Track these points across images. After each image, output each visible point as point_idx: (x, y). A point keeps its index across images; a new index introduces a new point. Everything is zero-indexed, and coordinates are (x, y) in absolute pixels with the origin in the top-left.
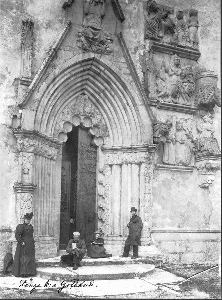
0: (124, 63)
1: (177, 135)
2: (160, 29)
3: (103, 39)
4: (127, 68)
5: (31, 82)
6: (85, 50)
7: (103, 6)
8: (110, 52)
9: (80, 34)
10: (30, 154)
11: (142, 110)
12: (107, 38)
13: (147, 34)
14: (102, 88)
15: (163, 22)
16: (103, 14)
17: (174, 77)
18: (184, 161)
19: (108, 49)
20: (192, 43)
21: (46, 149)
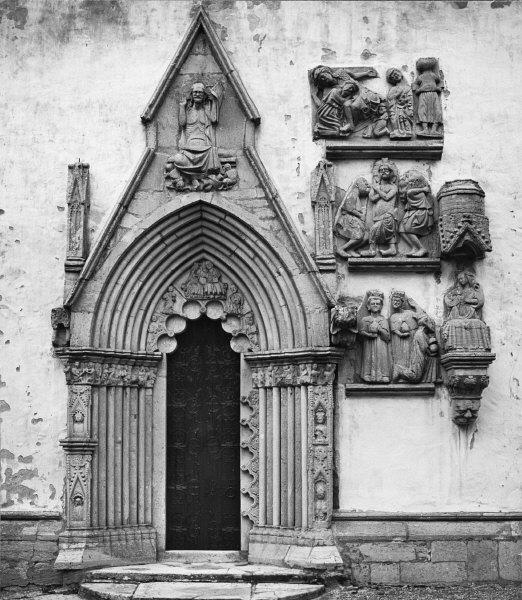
0: (260, 198)
1: (392, 319)
2: (343, 116)
3: (214, 162)
4: (268, 207)
5: (82, 266)
6: (180, 190)
7: (214, 106)
8: (232, 184)
9: (169, 166)
10: (84, 388)
11: (302, 282)
12: (225, 160)
13: (316, 130)
14: (233, 248)
15: (347, 103)
16: (214, 120)
17: (380, 203)
18: (407, 372)
19: (225, 180)
20: (425, 125)
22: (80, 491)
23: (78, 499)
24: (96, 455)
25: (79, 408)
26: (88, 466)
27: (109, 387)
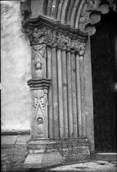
21: (66, 41)
22: (41, 113)
23: (40, 120)
24: (50, 90)
25: (38, 59)
26: (46, 96)
27: (57, 49)
